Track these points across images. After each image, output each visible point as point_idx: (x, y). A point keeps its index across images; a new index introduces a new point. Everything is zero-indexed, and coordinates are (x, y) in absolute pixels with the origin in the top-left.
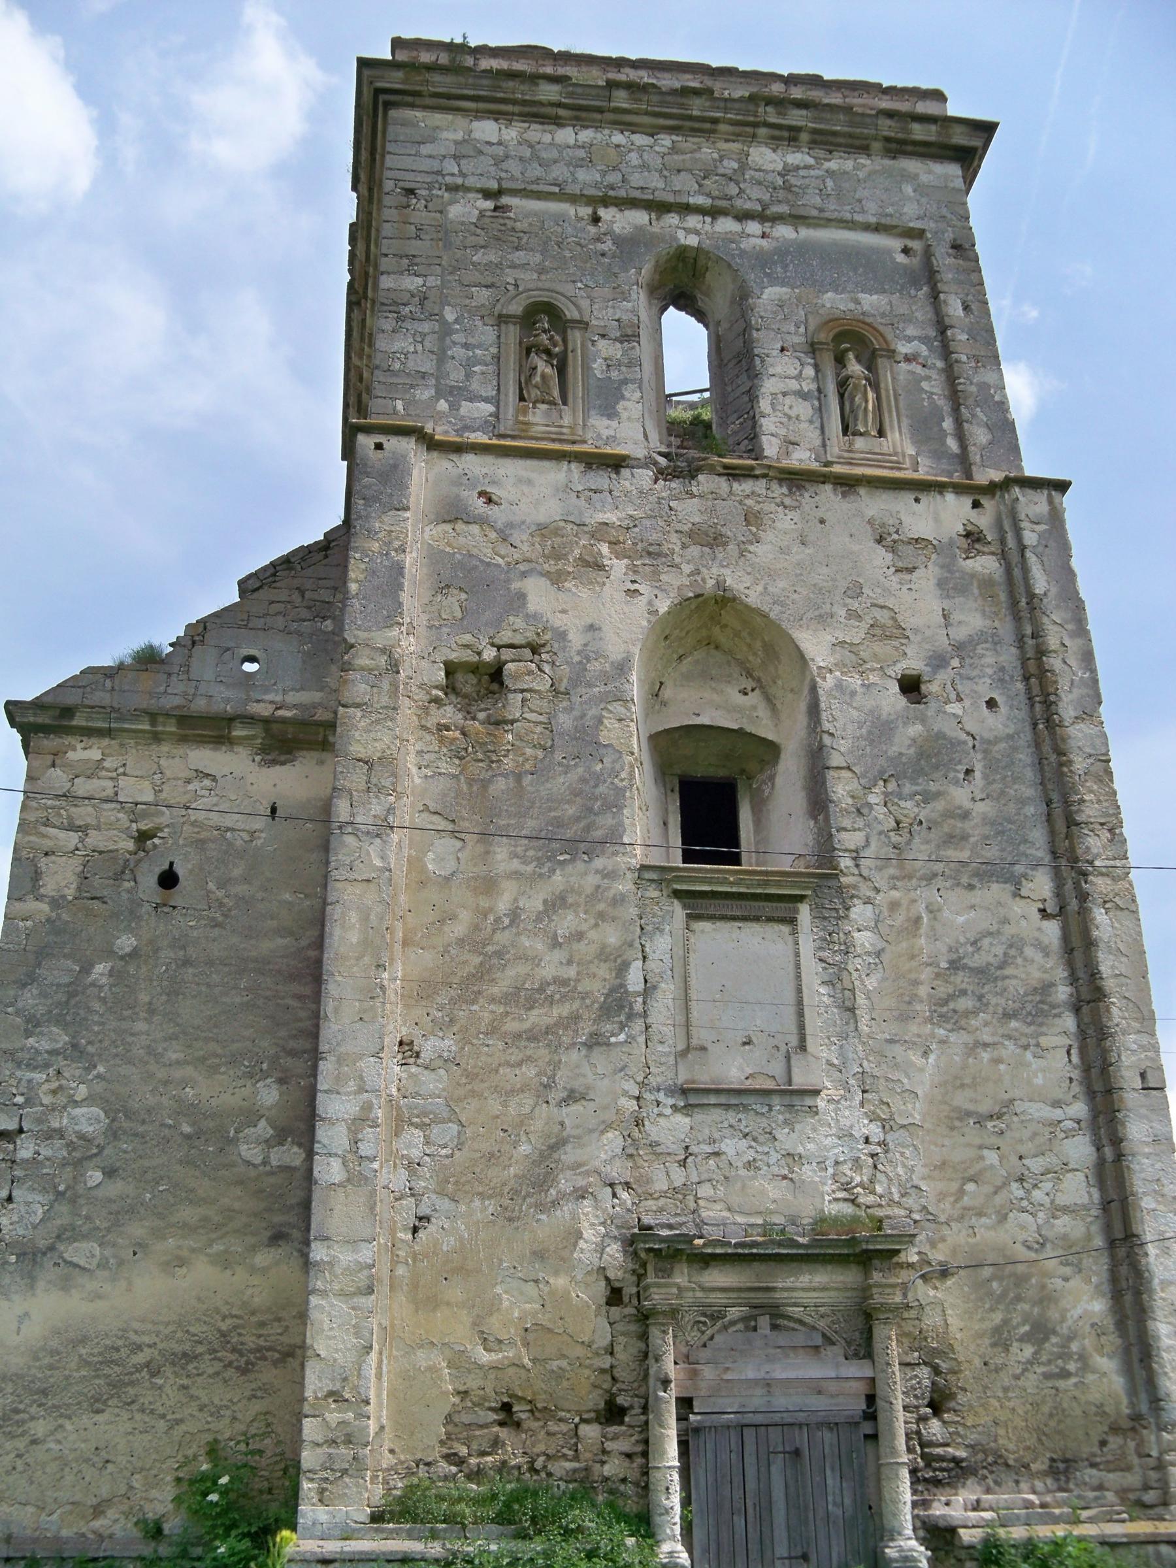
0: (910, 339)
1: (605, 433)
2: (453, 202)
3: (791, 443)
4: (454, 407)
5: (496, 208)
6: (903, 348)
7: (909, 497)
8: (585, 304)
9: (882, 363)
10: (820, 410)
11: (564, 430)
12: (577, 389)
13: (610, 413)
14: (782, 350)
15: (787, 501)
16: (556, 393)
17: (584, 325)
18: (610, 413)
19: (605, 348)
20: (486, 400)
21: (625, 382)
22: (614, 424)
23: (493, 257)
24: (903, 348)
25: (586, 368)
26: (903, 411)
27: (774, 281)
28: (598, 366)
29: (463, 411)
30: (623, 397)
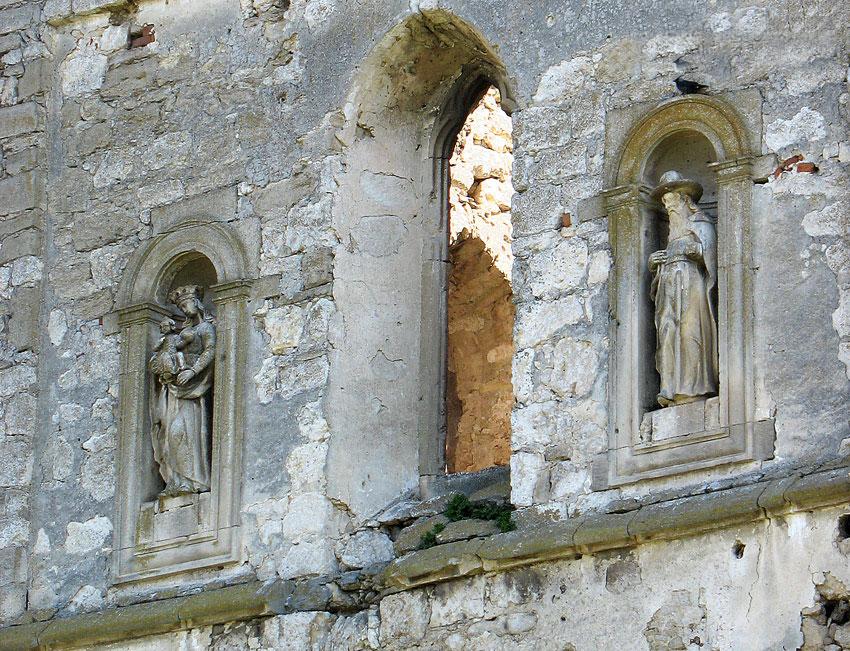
0: (790, 108)
1: (270, 529)
2: (65, 53)
3: (556, 457)
4: (58, 537)
5: (138, 38)
6: (776, 140)
7: (720, 546)
8: (247, 231)
9: (729, 195)
10: (610, 361)
11: (205, 547)
12: (226, 450)
13: (276, 481)
14: (564, 223)
15: (517, 622)
16: (193, 471)
17: (243, 286)
18: (276, 481)
19: (283, 327)
20: (100, 509)
21: (300, 400)
22: (279, 506)
23: (120, 171)
24: (776, 140)
25: (243, 384)
26: (760, 312)
27: (561, 46)
28: (262, 376)
29: (71, 545)
30: (298, 439)
